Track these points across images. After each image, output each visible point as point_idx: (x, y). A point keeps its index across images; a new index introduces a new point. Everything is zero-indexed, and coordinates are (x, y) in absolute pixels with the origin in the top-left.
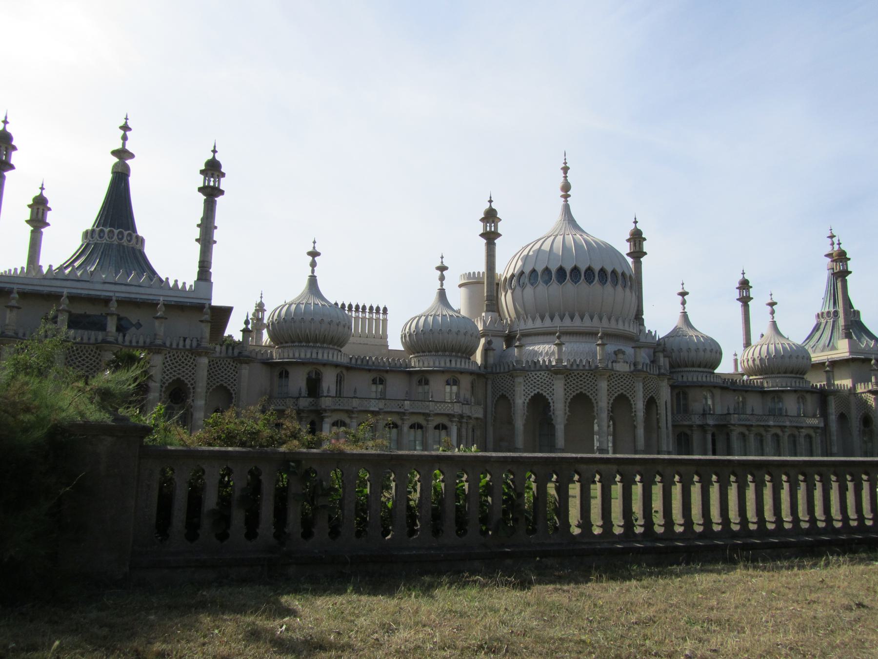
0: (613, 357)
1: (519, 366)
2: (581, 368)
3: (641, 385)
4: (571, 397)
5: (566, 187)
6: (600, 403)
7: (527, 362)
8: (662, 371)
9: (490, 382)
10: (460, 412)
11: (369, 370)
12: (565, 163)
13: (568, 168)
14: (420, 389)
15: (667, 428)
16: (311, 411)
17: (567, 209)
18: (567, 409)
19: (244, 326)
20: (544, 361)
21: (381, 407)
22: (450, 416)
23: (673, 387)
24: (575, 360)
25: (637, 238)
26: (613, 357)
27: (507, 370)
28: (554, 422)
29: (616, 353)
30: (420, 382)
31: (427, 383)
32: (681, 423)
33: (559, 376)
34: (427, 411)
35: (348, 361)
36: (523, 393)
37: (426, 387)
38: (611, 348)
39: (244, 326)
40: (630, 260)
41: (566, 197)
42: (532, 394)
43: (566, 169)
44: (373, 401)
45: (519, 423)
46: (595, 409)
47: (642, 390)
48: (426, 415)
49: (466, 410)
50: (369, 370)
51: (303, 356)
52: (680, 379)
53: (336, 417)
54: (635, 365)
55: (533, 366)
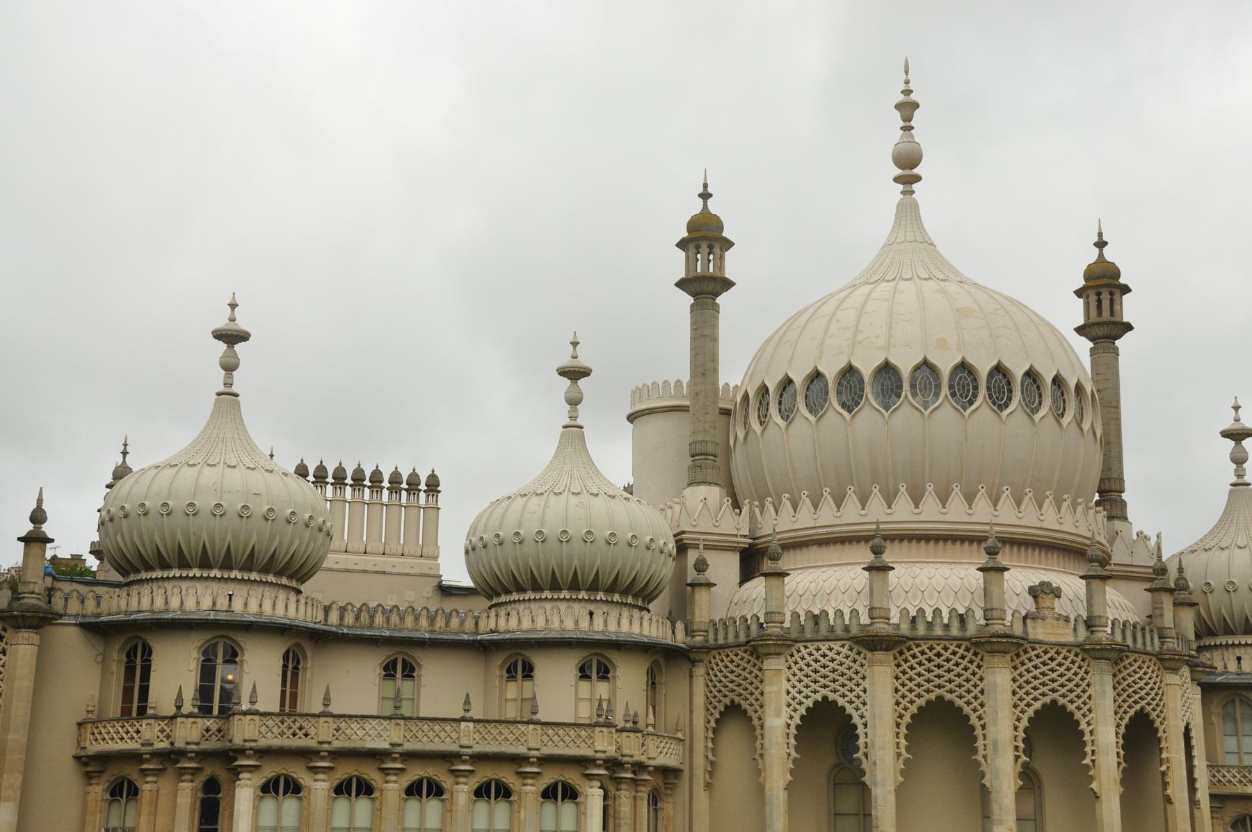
1: (774, 630)
2: (939, 632)
3: (1109, 680)
4: (913, 709)
6: (990, 729)
7: (795, 615)
8: (1171, 644)
9: (700, 671)
10: (611, 751)
11: (374, 642)
12: (907, 92)
13: (916, 106)
14: (512, 690)
15: (1193, 803)
16: (204, 755)
17: (908, 212)
18: (903, 742)
19: (30, 527)
20: (839, 613)
21: (396, 740)
22: (581, 762)
23: (1209, 690)
24: (921, 611)
25: (1103, 286)
26: (1029, 605)
27: (742, 639)
28: (867, 779)
29: (1034, 592)
30: (511, 673)
31: (528, 672)
32: (1240, 789)
33: (879, 655)
34: (521, 750)
35: (321, 617)
36: (785, 699)
37: (527, 684)
38: (1020, 577)
39: (30, 527)
40: (1083, 346)
41: (908, 180)
42: (810, 703)
43: (907, 109)
44: (374, 722)
45: (778, 775)
46: (980, 743)
47: (1110, 693)
48: (516, 760)
49: (632, 748)
50: (374, 642)
51: (190, 605)
52: (1232, 667)
53: (270, 770)
54: (1090, 624)
55: (809, 626)
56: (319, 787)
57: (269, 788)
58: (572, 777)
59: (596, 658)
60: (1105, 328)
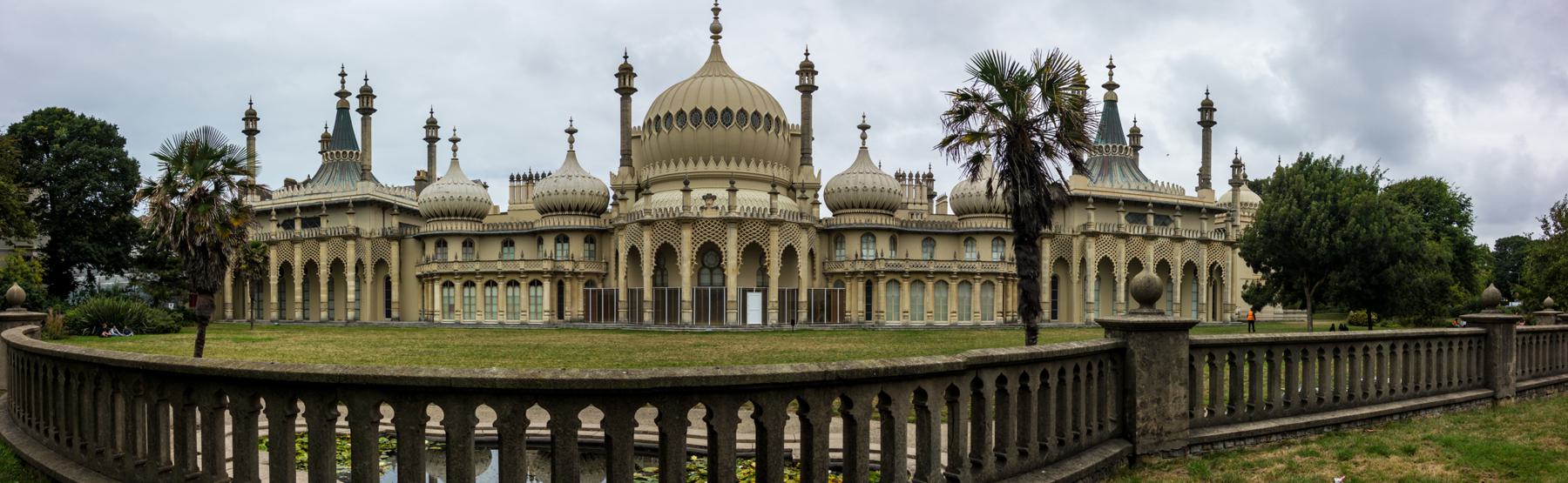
0: (703, 203)
5: (716, 31)
17: (716, 50)
22: (541, 273)
26: (703, 203)
29: (705, 198)
43: (716, 11)
56: (458, 284)
57: (445, 285)
58: (539, 278)
59: (562, 236)
60: (807, 90)
